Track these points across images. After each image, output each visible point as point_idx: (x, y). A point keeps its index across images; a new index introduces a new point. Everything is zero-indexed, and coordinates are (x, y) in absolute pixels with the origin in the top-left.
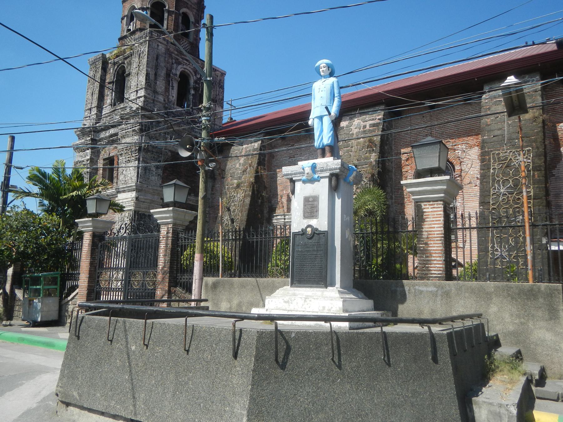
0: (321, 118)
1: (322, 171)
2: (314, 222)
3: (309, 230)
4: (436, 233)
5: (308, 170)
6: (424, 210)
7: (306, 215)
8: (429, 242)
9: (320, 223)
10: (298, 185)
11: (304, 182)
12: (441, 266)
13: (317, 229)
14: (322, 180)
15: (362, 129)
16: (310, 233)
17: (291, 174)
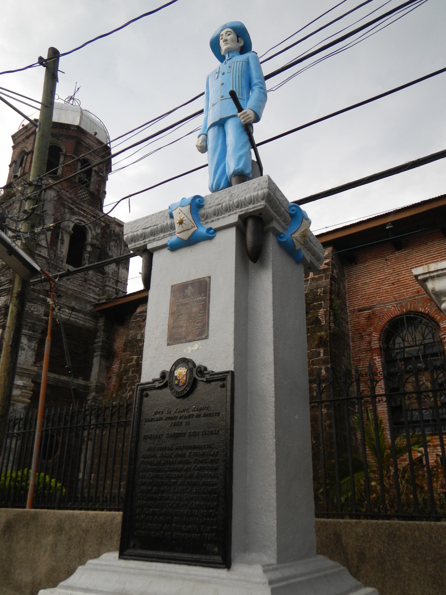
1: (217, 213)
2: (193, 351)
9: (215, 352)
11: (174, 247)
13: (202, 371)
14: (220, 236)
17: (144, 236)
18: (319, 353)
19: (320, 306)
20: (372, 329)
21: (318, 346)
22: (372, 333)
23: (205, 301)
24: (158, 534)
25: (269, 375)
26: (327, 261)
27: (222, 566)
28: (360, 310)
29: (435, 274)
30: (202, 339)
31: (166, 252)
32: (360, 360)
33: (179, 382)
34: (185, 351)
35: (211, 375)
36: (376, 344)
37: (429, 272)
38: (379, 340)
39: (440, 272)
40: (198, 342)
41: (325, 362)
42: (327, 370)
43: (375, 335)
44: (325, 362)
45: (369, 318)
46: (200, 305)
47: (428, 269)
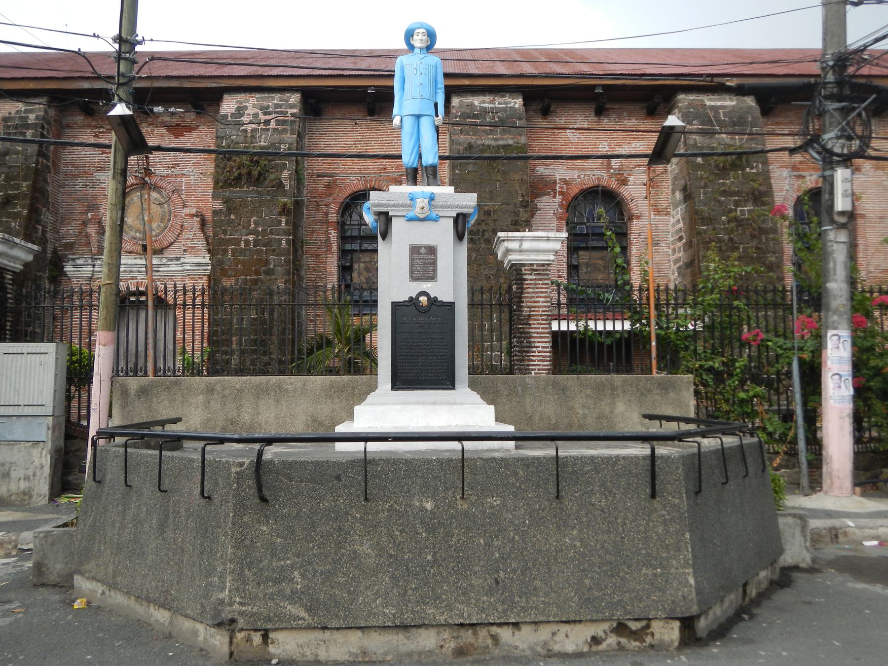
0: (418, 117)
3: (423, 299)
4: (541, 309)
5: (421, 202)
6: (526, 277)
7: (416, 275)
8: (531, 322)
10: (397, 225)
11: (410, 220)
12: (548, 354)
14: (442, 220)
16: (425, 303)
18: (280, 221)
19: (284, 167)
20: (331, 200)
21: (280, 214)
22: (330, 204)
26: (295, 111)
28: (319, 176)
31: (403, 220)
32: (313, 232)
36: (333, 217)
38: (338, 213)
41: (286, 233)
42: (288, 242)
43: (334, 208)
44: (286, 233)
45: (328, 186)
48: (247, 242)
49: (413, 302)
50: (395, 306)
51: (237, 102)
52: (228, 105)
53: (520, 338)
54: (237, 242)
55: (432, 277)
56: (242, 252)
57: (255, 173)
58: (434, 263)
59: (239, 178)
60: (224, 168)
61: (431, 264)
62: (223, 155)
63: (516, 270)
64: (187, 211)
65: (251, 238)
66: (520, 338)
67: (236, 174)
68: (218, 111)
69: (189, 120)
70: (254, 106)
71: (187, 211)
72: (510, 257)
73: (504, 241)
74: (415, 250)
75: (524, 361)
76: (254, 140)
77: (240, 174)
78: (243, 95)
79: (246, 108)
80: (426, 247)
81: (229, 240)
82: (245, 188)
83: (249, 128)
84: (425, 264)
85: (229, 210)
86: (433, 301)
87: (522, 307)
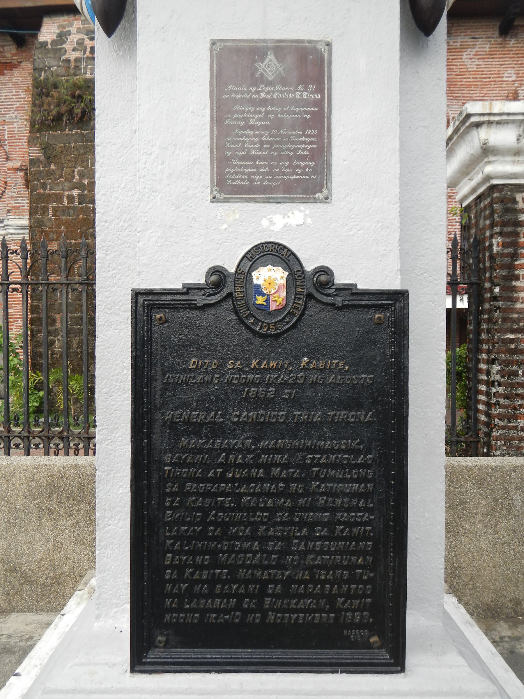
3: (270, 278)
13: (324, 276)
15: (88, 53)
16: (279, 299)
23: (319, 103)
24: (227, 617)
25: (436, 294)
27: (394, 669)
29: (497, 118)
30: (315, 201)
33: (267, 301)
34: (265, 223)
35: (353, 294)
37: (490, 114)
39: (505, 117)
40: (302, 207)
46: (306, 112)
47: (490, 109)
48: (71, 198)
49: (226, 288)
50: (149, 308)
51: (58, 27)
52: (49, 31)
53: (508, 363)
54: (59, 198)
55: (305, 176)
56: (65, 210)
57: (78, 111)
58: (318, 121)
59: (58, 118)
60: (40, 106)
61: (305, 125)
62: (41, 90)
63: (502, 201)
64: (10, 164)
65: (75, 193)
66: (508, 363)
67: (54, 112)
68: (35, 36)
69: (8, 55)
70: (79, 31)
71: (10, 164)
72: (489, 169)
73: (478, 125)
74: (235, 64)
75: (516, 418)
76: (78, 72)
77: (59, 113)
78: (66, 18)
79: (69, 33)
80: (280, 48)
81: (49, 195)
82: (67, 130)
83: (72, 56)
84: (279, 124)
85: (49, 159)
86: (314, 288)
87: (514, 289)
